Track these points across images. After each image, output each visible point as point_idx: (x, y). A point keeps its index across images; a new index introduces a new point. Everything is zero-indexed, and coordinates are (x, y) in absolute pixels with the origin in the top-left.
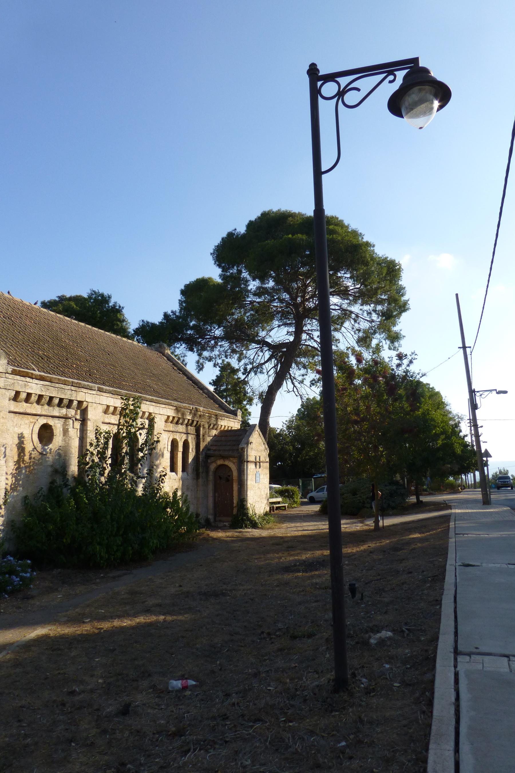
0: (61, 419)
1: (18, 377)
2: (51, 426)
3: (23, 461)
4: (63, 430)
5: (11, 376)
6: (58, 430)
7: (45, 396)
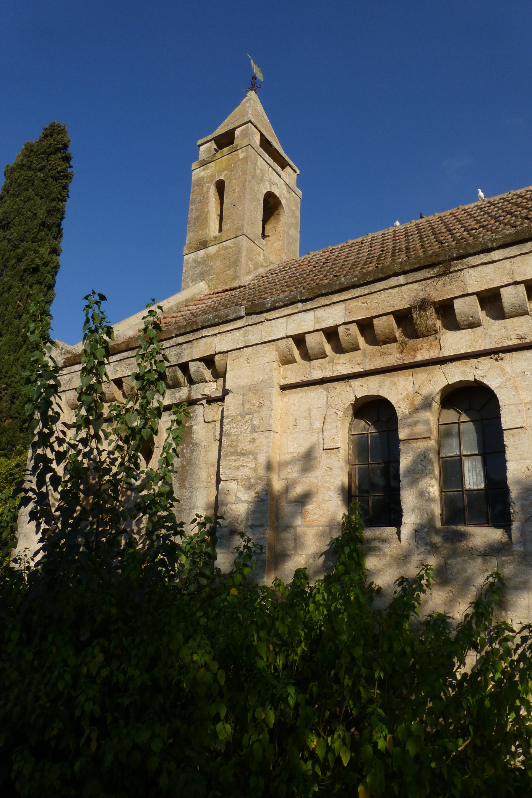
7: (124, 379)
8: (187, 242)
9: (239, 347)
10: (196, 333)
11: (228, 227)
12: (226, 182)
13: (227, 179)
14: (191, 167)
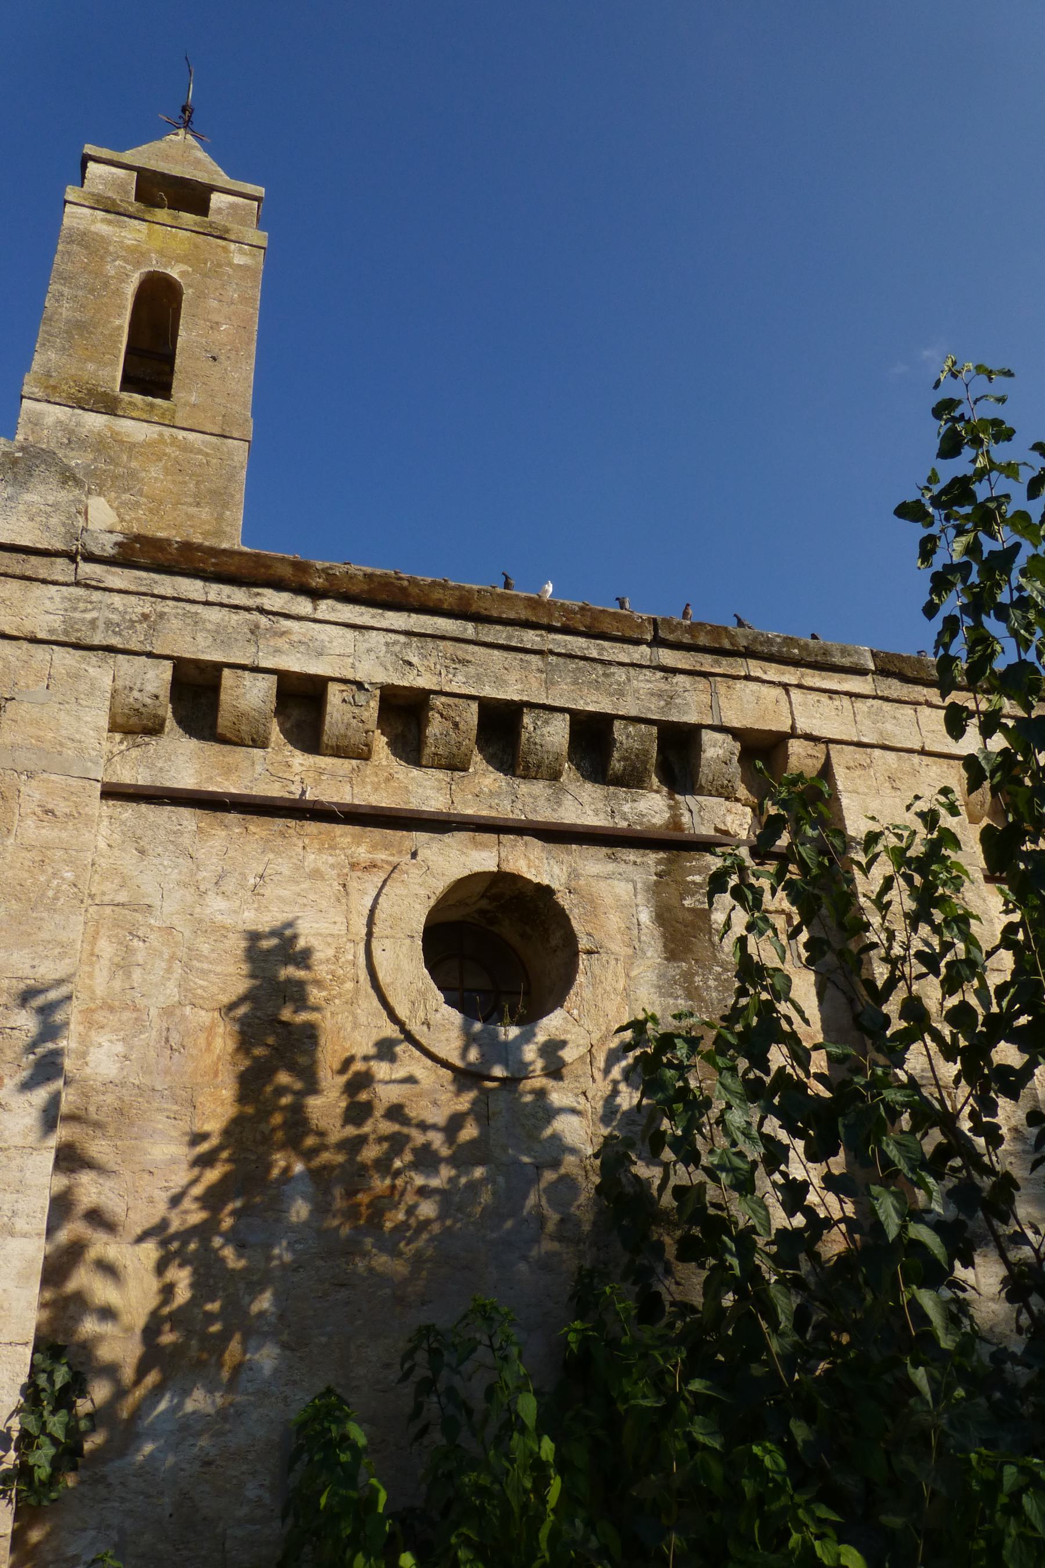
0: (632, 855)
1: (193, 587)
2: (546, 892)
3: (298, 1123)
4: (663, 917)
5: (118, 577)
6: (614, 921)
7: (438, 701)
8: (35, 366)
9: (865, 740)
10: (724, 661)
12: (188, 293)
13: (190, 286)
14: (64, 192)
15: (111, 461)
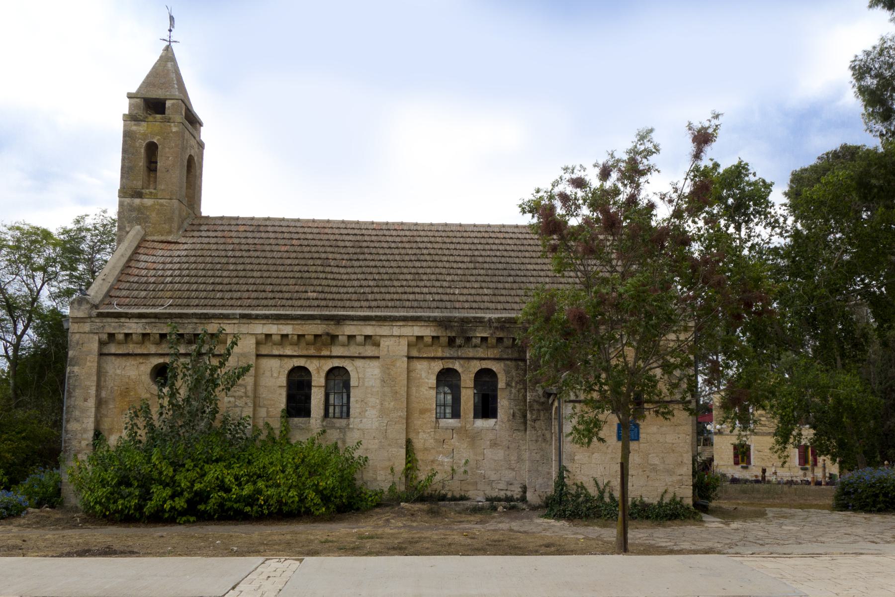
11: (163, 187)
12: (160, 147)
15: (142, 213)
